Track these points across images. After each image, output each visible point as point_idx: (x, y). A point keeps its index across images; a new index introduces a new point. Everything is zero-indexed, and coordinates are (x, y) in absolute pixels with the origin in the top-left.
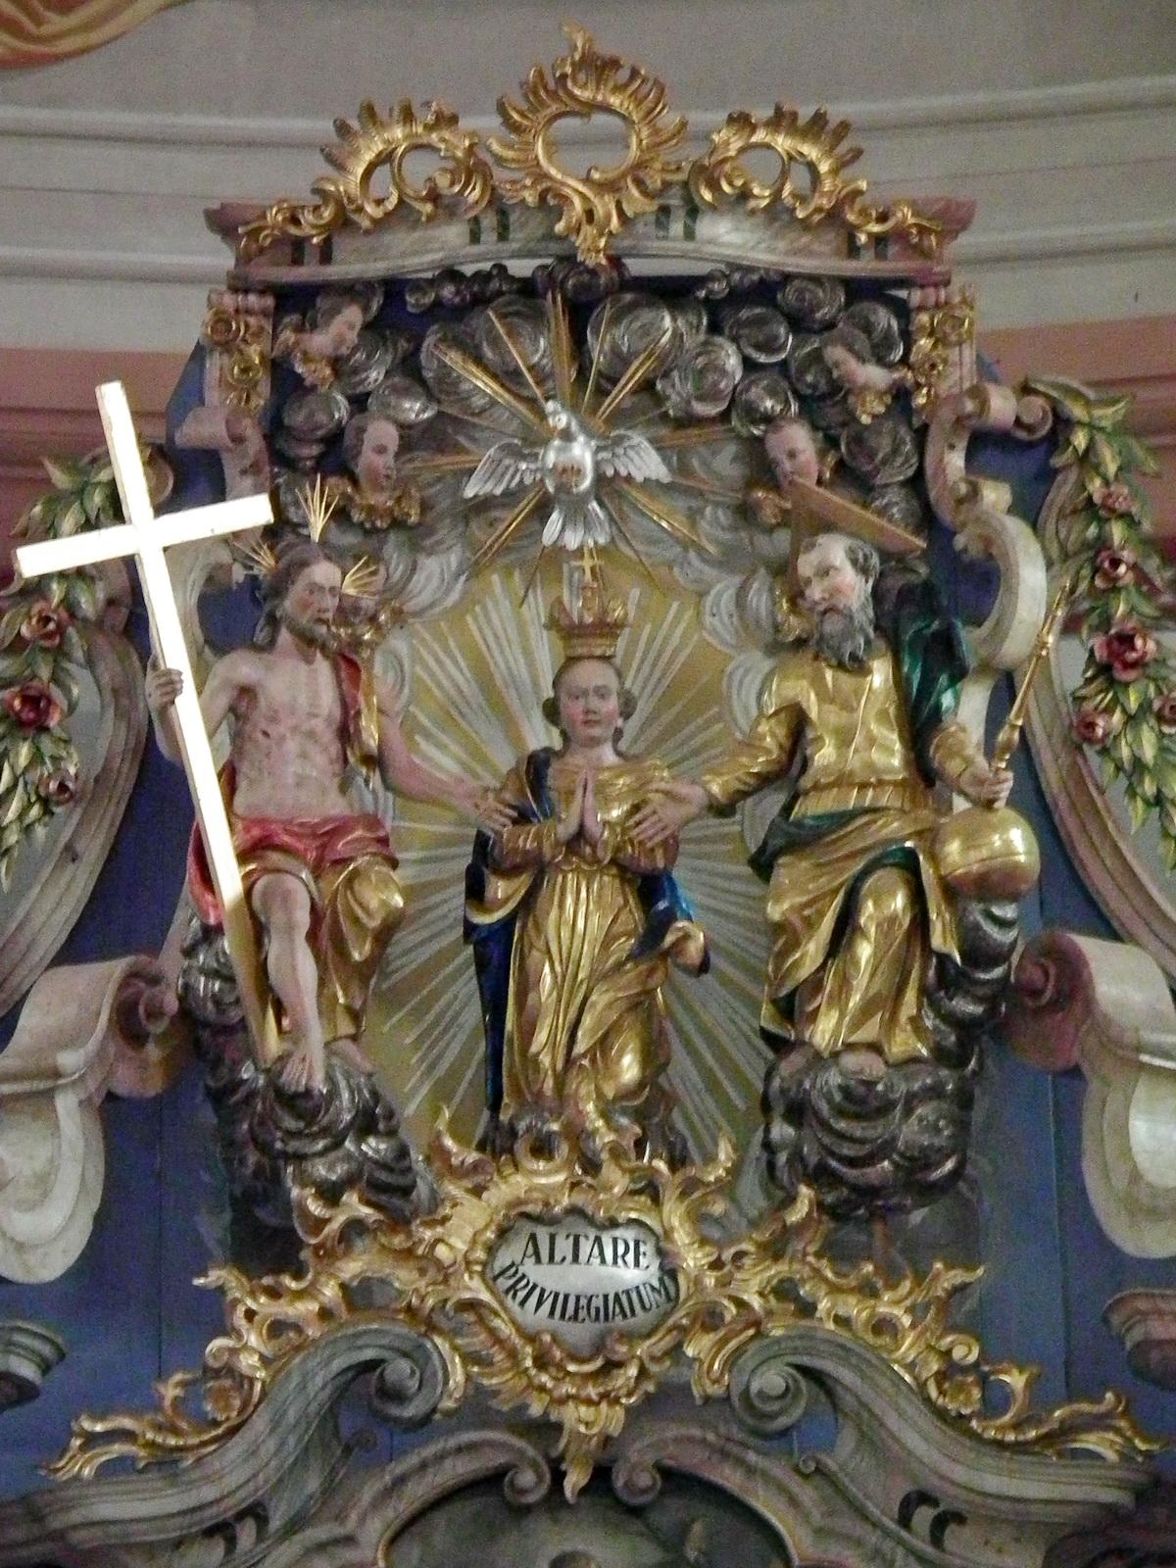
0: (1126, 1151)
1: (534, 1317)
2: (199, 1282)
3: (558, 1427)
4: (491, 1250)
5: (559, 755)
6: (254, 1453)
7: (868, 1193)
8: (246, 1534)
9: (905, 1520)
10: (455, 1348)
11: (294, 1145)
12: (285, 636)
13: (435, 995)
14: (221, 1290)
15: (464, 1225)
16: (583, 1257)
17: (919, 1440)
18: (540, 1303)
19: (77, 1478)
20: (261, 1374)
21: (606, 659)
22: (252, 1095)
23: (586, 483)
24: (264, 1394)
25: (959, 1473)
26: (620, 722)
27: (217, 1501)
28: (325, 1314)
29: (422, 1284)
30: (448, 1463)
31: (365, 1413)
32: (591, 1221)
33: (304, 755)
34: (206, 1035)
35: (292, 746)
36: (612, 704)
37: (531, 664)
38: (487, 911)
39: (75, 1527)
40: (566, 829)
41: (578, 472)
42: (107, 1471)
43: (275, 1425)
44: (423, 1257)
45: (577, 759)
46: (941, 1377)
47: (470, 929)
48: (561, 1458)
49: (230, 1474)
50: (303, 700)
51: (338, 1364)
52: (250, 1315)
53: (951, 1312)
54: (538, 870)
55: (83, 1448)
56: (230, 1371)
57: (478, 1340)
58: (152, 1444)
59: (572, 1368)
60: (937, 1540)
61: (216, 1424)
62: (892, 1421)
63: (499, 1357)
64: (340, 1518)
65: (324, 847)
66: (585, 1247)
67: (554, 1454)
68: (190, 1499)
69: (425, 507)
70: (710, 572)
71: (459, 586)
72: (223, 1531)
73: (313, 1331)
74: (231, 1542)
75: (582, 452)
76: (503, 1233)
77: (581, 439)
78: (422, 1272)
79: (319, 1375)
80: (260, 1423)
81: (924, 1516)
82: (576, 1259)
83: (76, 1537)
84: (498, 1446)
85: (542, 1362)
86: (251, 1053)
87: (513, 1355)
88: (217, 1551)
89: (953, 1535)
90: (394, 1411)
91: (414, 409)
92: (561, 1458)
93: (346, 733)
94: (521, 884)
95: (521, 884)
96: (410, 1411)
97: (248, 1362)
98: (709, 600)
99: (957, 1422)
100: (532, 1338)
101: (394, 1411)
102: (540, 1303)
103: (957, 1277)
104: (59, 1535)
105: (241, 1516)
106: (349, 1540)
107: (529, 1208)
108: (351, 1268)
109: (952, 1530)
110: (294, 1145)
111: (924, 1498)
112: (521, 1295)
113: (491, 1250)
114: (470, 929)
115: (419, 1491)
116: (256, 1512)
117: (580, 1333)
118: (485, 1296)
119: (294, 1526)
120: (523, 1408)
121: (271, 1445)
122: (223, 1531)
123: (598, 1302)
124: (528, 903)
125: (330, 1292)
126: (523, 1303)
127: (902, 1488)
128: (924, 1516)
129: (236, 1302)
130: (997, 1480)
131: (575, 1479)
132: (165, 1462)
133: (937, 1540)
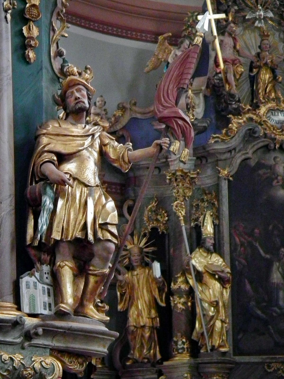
1: (273, 123)
2: (228, 116)
3: (275, 139)
4: (267, 114)
5: (261, 53)
6: (236, 140)
8: (233, 152)
10: (262, 127)
11: (231, 102)
12: (226, 34)
13: (241, 87)
14: (231, 118)
15: (263, 110)
16: (279, 115)
18: (273, 121)
19: (211, 143)
20: (236, 130)
21: (268, 40)
22: (225, 95)
23: (262, 17)
24: (237, 132)
26: (269, 49)
27: (231, 147)
28: (244, 122)
29: (257, 118)
30: (260, 143)
31: (251, 135)
32: (280, 110)
33: (229, 50)
34: (216, 88)
35: (228, 48)
36: (268, 46)
37: (252, 42)
38: (253, 73)
39: (211, 150)
40: (264, 62)
41: (261, 15)
42: (216, 142)
43: (239, 136)
44: (257, 115)
45: (263, 53)
47: (250, 75)
48: (275, 143)
49: (233, 143)
50: (229, 43)
51: (246, 129)
52: (234, 122)
54: (259, 68)
55: (213, 139)
56: (232, 129)
57: (264, 126)
58: (222, 139)
59: (278, 131)
61: (230, 136)
63: (267, 129)
64: (246, 150)
65: (234, 62)
66: (279, 114)
67: (275, 142)
68: (227, 146)
69: (238, 21)
70: (275, 32)
71: (242, 32)
72: (230, 151)
73: (243, 124)
74: (231, 153)
75: (262, 13)
76: (268, 111)
77: (262, 11)
78: (257, 117)
79: (243, 131)
80: (237, 136)
82: (278, 115)
83: (210, 151)
84: (266, 141)
85: (274, 129)
86: (224, 90)
87: (270, 128)
88: (229, 154)
90: (254, 135)
91: (236, 8)
92: (275, 143)
93: (235, 47)
94: (257, 70)
95: (257, 70)
96: (256, 135)
97: (234, 128)
98: (275, 36)
100: (272, 126)
101: (254, 135)
102: (273, 121)
104: (208, 151)
105: (233, 149)
106: (247, 153)
107: (271, 108)
108: (247, 116)
110: (231, 102)
112: (271, 120)
113: (267, 114)
114: (250, 75)
115: (256, 148)
116: (235, 149)
117: (279, 126)
118: (266, 120)
119: (240, 151)
120: (271, 135)
121: (238, 139)
122: (230, 151)
123: (281, 122)
124: (258, 73)
125: (245, 119)
126: (271, 121)
129: (233, 120)
131: (277, 146)
132: (223, 141)
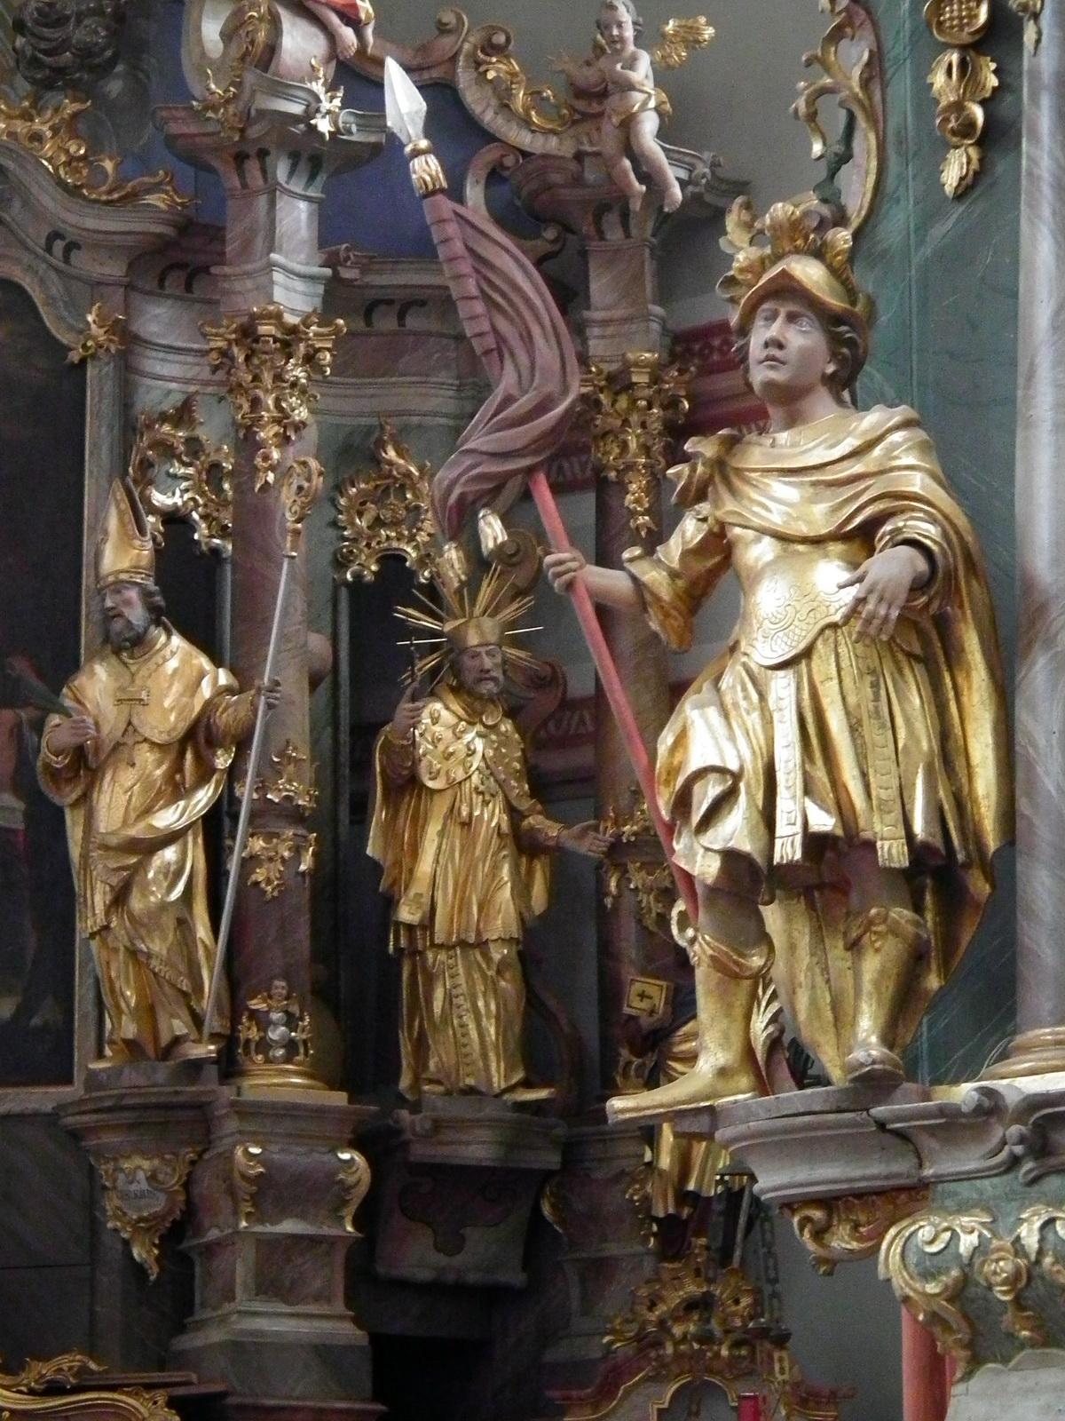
0: (200, 41)
7: (60, 71)
9: (49, 249)
17: (49, 200)
25: (72, 219)
46: (68, 164)
53: (71, 127)
60: (66, 259)
62: (35, 190)
81: (59, 246)
89: (75, 256)
99: (73, 191)
103: (76, 107)
109: (74, 255)
111: (55, 235)
127: (45, 231)
128: (59, 246)
130: (92, 221)
133: (66, 259)
